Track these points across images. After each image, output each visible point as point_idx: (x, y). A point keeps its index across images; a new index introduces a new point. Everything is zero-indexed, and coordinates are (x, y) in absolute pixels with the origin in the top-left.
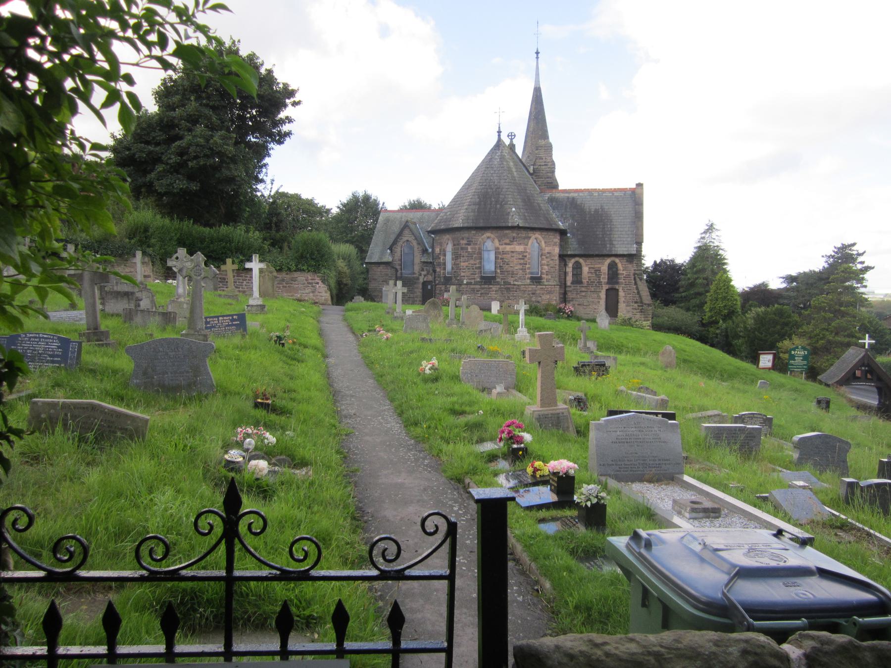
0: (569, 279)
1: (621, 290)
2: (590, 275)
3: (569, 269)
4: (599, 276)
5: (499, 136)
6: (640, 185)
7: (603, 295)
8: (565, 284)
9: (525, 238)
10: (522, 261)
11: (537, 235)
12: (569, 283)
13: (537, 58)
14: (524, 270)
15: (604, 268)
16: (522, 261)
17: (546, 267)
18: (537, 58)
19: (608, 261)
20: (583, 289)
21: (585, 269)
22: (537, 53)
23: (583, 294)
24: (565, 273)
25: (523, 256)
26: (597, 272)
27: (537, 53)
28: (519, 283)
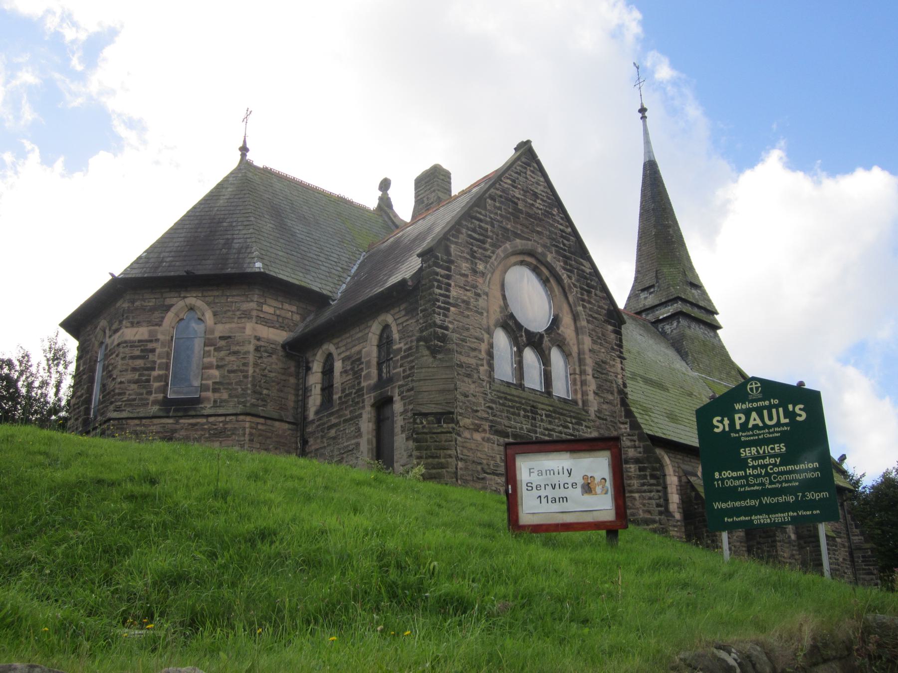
0: (315, 400)
1: (396, 398)
2: (345, 378)
3: (315, 379)
4: (357, 375)
5: (243, 155)
6: (526, 154)
7: (367, 425)
8: (305, 418)
9: (153, 309)
10: (139, 363)
11: (192, 300)
12: (311, 415)
13: (644, 118)
14: (143, 383)
15: (370, 350)
16: (139, 363)
17: (215, 373)
18: (644, 118)
19: (375, 328)
20: (334, 420)
21: (338, 366)
22: (643, 110)
23: (333, 433)
24: (306, 391)
25: (145, 349)
26: (355, 363)
27: (643, 110)
28: (124, 415)
